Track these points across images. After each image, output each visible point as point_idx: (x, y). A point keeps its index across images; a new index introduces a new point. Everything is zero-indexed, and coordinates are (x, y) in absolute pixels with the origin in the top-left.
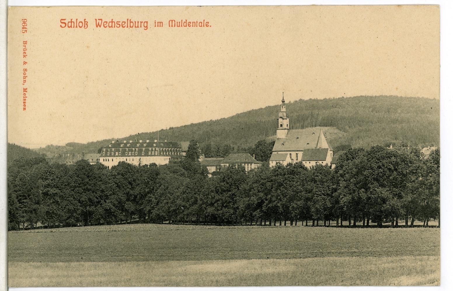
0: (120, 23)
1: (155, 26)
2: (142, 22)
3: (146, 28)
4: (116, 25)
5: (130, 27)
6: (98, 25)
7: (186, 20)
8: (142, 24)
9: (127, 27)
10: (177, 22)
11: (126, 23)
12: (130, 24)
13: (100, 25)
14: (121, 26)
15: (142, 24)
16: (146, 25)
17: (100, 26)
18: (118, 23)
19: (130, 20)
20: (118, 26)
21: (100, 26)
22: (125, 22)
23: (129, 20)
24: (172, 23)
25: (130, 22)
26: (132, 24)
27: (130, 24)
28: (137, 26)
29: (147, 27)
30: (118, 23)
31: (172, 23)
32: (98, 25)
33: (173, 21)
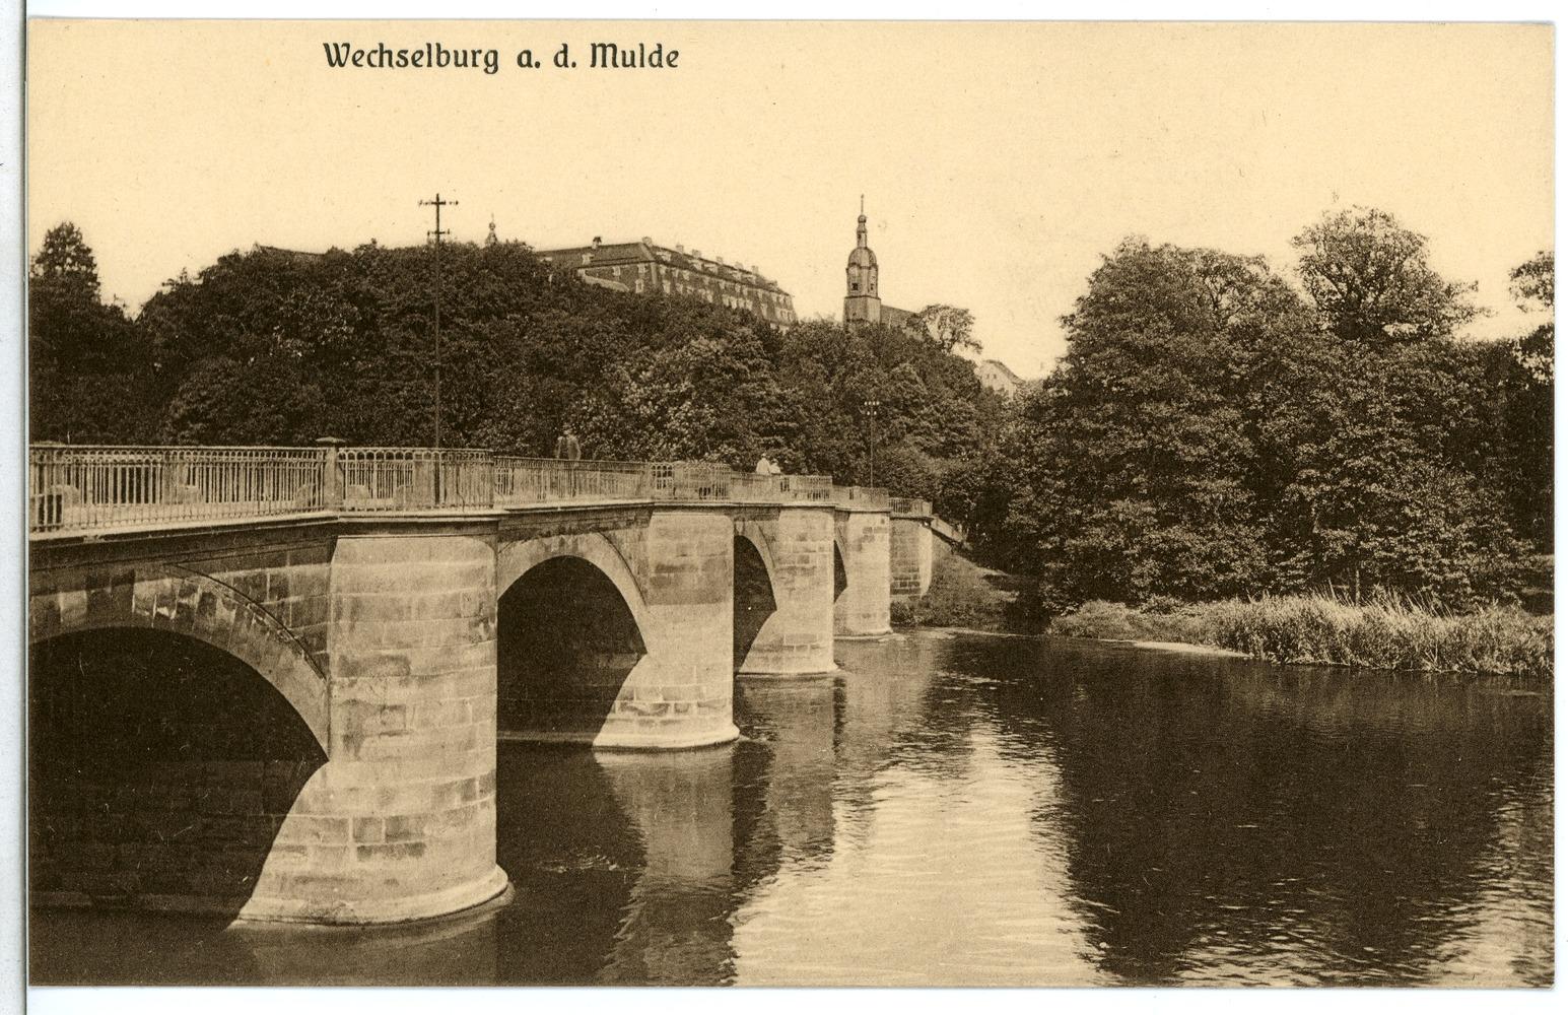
0: (409, 56)
1: (593, 65)
4: (395, 58)
6: (335, 61)
7: (660, 46)
9: (430, 65)
10: (624, 53)
12: (436, 55)
20: (402, 62)
21: (342, 65)
22: (421, 53)
24: (604, 53)
26: (443, 57)
27: (436, 55)
28: (461, 61)
31: (604, 53)
32: (335, 61)
33: (610, 51)
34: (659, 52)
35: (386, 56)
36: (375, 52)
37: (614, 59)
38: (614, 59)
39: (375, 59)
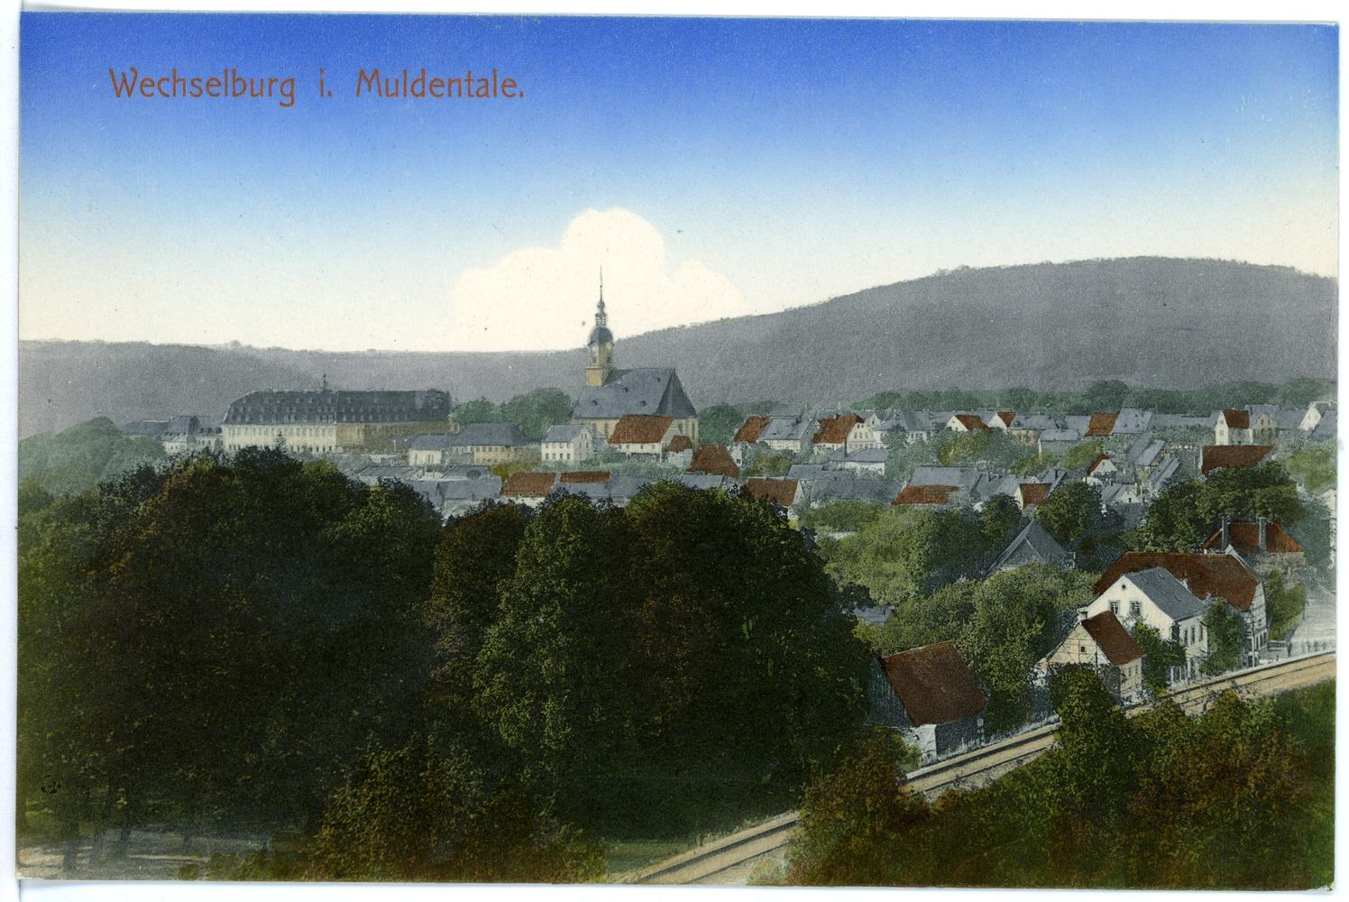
2: (276, 80)
3: (287, 100)
5: (235, 95)
8: (276, 87)
11: (223, 81)
13: (130, 86)
14: (204, 91)
15: (276, 87)
16: (287, 90)
17: (130, 94)
18: (196, 83)
19: (234, 72)
20: (196, 91)
23: (230, 77)
25: (235, 80)
29: (291, 95)
30: (196, 83)
34: (423, 80)
35: (179, 86)
36: (168, 80)
37: (405, 91)
38: (405, 91)
39: (166, 87)
